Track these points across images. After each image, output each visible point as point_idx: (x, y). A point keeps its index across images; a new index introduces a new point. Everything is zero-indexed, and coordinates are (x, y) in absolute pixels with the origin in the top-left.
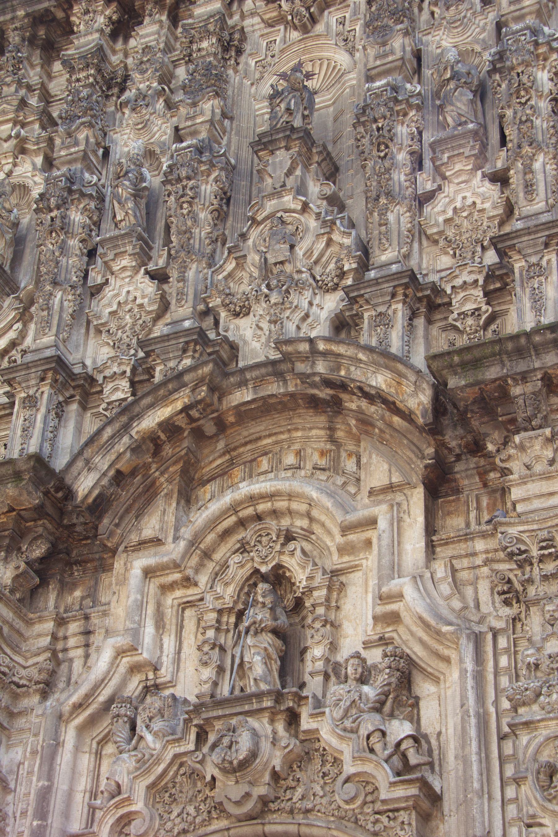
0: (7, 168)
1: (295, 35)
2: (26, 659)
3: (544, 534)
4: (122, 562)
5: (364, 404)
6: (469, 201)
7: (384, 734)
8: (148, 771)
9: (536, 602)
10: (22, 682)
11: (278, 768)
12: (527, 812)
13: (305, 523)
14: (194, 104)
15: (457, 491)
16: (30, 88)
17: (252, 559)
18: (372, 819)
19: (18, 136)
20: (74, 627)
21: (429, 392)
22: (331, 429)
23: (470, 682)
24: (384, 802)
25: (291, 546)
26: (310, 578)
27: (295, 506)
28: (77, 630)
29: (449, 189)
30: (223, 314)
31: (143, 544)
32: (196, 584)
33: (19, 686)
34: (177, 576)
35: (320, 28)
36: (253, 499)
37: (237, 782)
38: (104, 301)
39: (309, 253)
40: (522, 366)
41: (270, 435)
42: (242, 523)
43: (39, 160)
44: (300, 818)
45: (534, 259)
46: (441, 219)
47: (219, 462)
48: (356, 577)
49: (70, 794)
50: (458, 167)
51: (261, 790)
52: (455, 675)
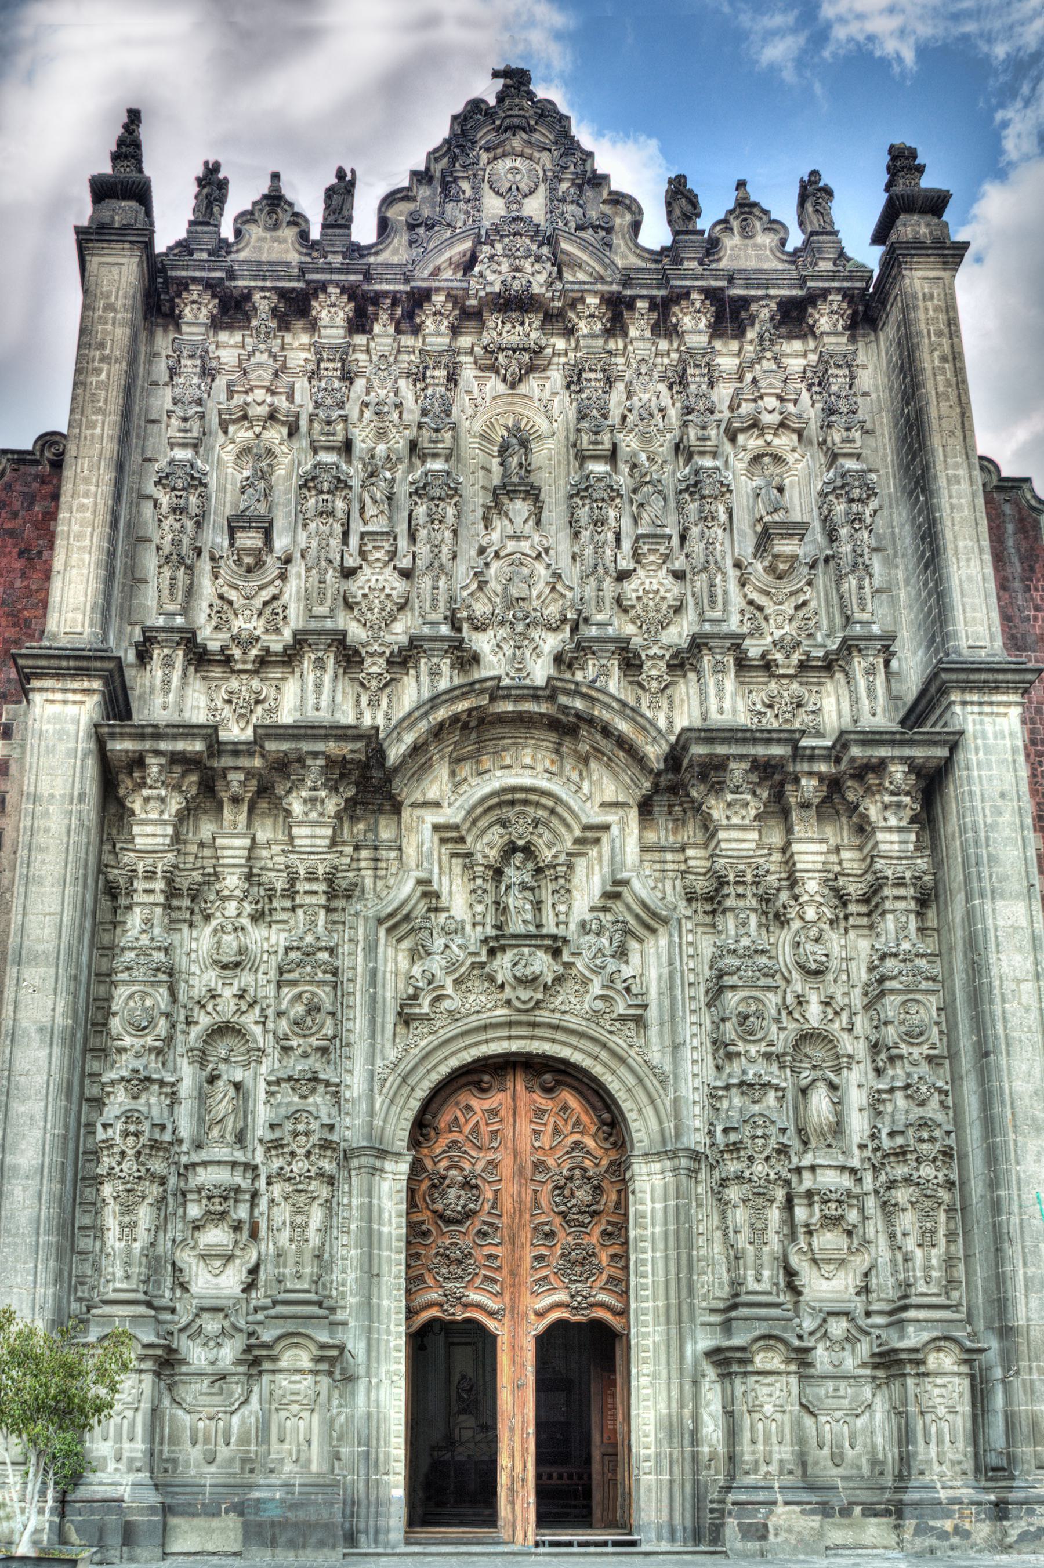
0: (258, 429)
6: (655, 587)
15: (650, 813)
20: (364, 854)
25: (541, 829)
26: (555, 857)
27: (543, 801)
29: (641, 572)
31: (426, 804)
34: (455, 834)
36: (514, 789)
39: (539, 597)
42: (499, 805)
43: (285, 431)
44: (558, 1015)
46: (634, 595)
50: (652, 558)
51: (540, 996)
52: (663, 941)
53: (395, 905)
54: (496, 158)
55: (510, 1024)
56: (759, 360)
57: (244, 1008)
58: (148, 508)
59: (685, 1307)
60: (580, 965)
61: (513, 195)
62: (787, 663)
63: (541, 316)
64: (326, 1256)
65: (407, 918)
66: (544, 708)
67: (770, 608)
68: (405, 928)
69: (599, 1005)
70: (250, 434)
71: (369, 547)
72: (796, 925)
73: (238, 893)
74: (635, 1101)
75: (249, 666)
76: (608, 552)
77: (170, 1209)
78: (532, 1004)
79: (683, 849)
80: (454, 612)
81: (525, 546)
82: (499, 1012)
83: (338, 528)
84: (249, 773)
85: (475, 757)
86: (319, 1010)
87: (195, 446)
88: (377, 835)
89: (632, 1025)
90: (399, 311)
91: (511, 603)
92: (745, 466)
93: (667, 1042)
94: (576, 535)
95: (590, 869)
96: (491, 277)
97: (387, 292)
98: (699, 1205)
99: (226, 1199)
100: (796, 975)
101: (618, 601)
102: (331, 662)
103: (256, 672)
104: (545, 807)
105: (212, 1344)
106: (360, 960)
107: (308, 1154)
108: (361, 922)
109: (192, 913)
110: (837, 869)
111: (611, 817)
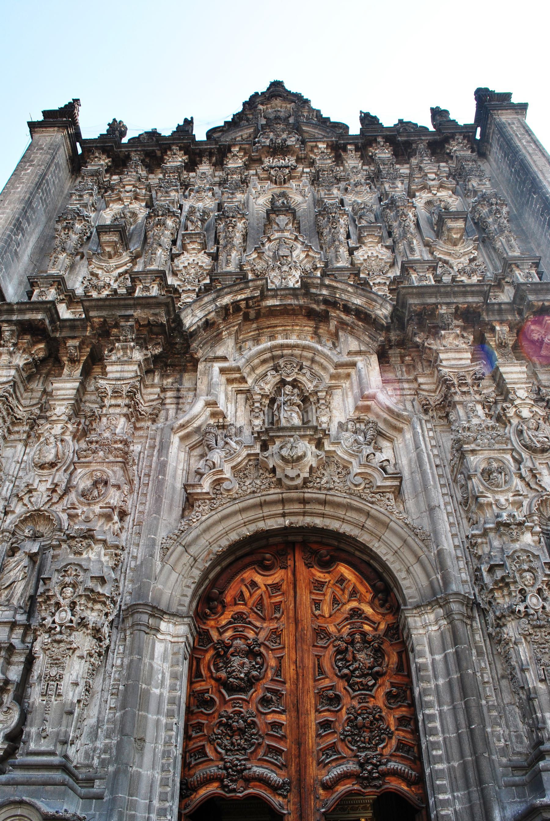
0: (126, 204)
2: (145, 402)
3: (461, 374)
4: (203, 366)
6: (375, 254)
7: (374, 455)
8: (232, 460)
9: (461, 403)
10: (142, 413)
11: (314, 465)
12: (478, 490)
14: (233, 194)
15: (388, 362)
17: (281, 375)
18: (370, 495)
19: (135, 191)
20: (169, 394)
21: (390, 308)
22: (317, 328)
23: (421, 438)
24: (378, 487)
27: (305, 353)
28: (172, 395)
32: (246, 382)
33: (141, 414)
34: (238, 375)
37: (292, 468)
40: (448, 300)
41: (282, 326)
43: (144, 204)
45: (421, 274)
46: (362, 258)
47: (252, 333)
48: (338, 392)
49: (176, 468)
50: (370, 240)
51: (307, 475)
52: (408, 436)
53: (187, 418)
55: (283, 502)
57: (55, 500)
59: (484, 764)
60: (339, 453)
63: (295, 158)
69: (359, 480)
71: (188, 241)
72: (515, 421)
73: (64, 417)
74: (402, 561)
78: (299, 481)
79: (416, 379)
82: (272, 491)
86: (106, 483)
89: (391, 496)
92: (423, 205)
93: (423, 507)
95: (344, 395)
97: (207, 149)
98: (480, 654)
100: (525, 455)
104: (307, 359)
106: (155, 458)
108: (159, 433)
109: (29, 436)
111: (358, 359)
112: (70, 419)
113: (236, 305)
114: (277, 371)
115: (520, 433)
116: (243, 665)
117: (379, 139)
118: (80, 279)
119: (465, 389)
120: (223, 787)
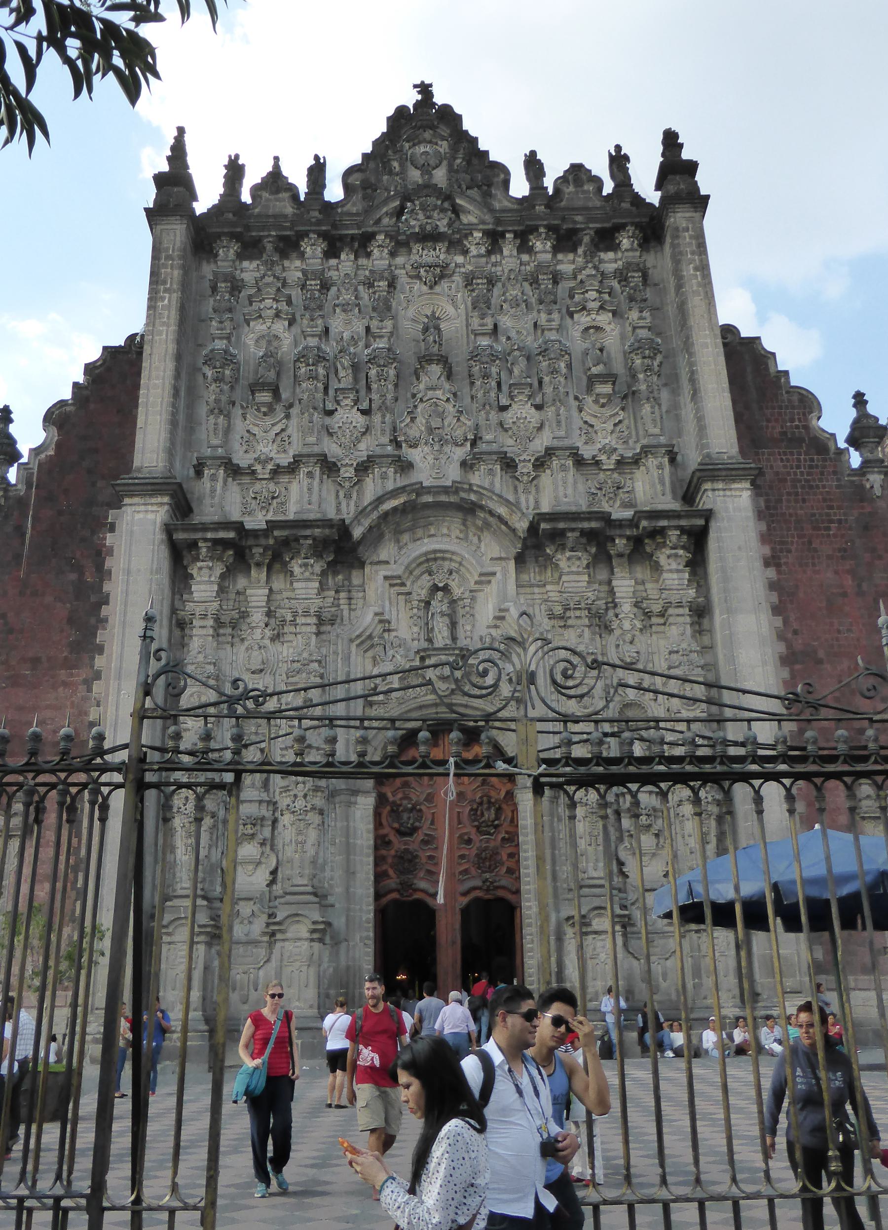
0: (268, 324)
1: (425, 289)
5: (487, 516)
13: (457, 565)
16: (278, 279)
19: (277, 309)
20: (343, 595)
27: (454, 557)
29: (514, 406)
30: (404, 445)
31: (380, 563)
35: (438, 289)
36: (435, 551)
38: (335, 420)
39: (449, 425)
42: (428, 561)
45: (563, 462)
50: (521, 398)
53: (361, 630)
54: (414, 145)
56: (584, 269)
58: (200, 379)
61: (426, 169)
62: (609, 463)
63: (446, 244)
64: (320, 861)
65: (370, 637)
66: (453, 499)
67: (598, 425)
68: (369, 643)
70: (264, 327)
71: (341, 397)
72: (617, 632)
75: (267, 476)
76: (493, 394)
77: (220, 832)
79: (544, 585)
80: (396, 438)
81: (439, 393)
83: (320, 386)
84: (266, 548)
85: (412, 529)
87: (228, 338)
88: (350, 582)
90: (356, 245)
91: (430, 430)
94: (472, 384)
96: (413, 223)
99: (254, 825)
101: (501, 424)
102: (317, 471)
103: (272, 479)
105: (246, 922)
107: (305, 796)
110: (644, 594)
111: (497, 569)
112: (267, 625)
113: (395, 509)
114: (430, 575)
115: (618, 646)
116: (409, 818)
117: (542, 230)
118: (238, 437)
119: (578, 613)
120: (401, 895)
